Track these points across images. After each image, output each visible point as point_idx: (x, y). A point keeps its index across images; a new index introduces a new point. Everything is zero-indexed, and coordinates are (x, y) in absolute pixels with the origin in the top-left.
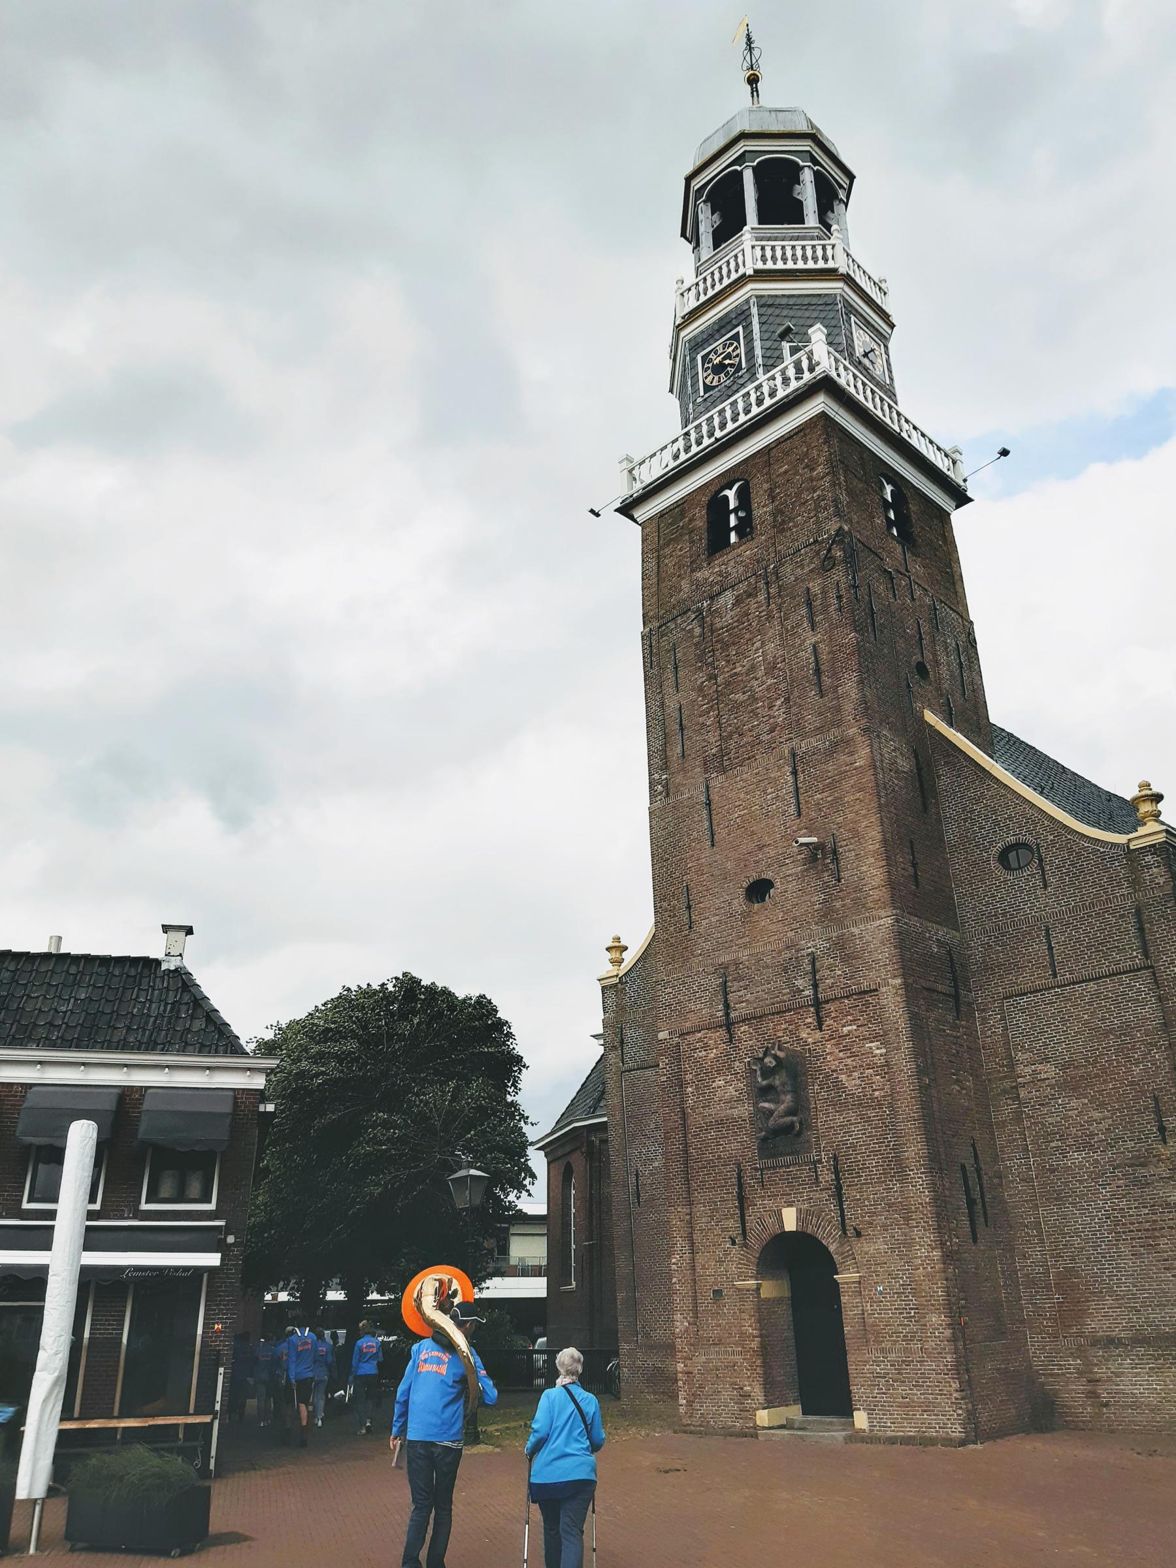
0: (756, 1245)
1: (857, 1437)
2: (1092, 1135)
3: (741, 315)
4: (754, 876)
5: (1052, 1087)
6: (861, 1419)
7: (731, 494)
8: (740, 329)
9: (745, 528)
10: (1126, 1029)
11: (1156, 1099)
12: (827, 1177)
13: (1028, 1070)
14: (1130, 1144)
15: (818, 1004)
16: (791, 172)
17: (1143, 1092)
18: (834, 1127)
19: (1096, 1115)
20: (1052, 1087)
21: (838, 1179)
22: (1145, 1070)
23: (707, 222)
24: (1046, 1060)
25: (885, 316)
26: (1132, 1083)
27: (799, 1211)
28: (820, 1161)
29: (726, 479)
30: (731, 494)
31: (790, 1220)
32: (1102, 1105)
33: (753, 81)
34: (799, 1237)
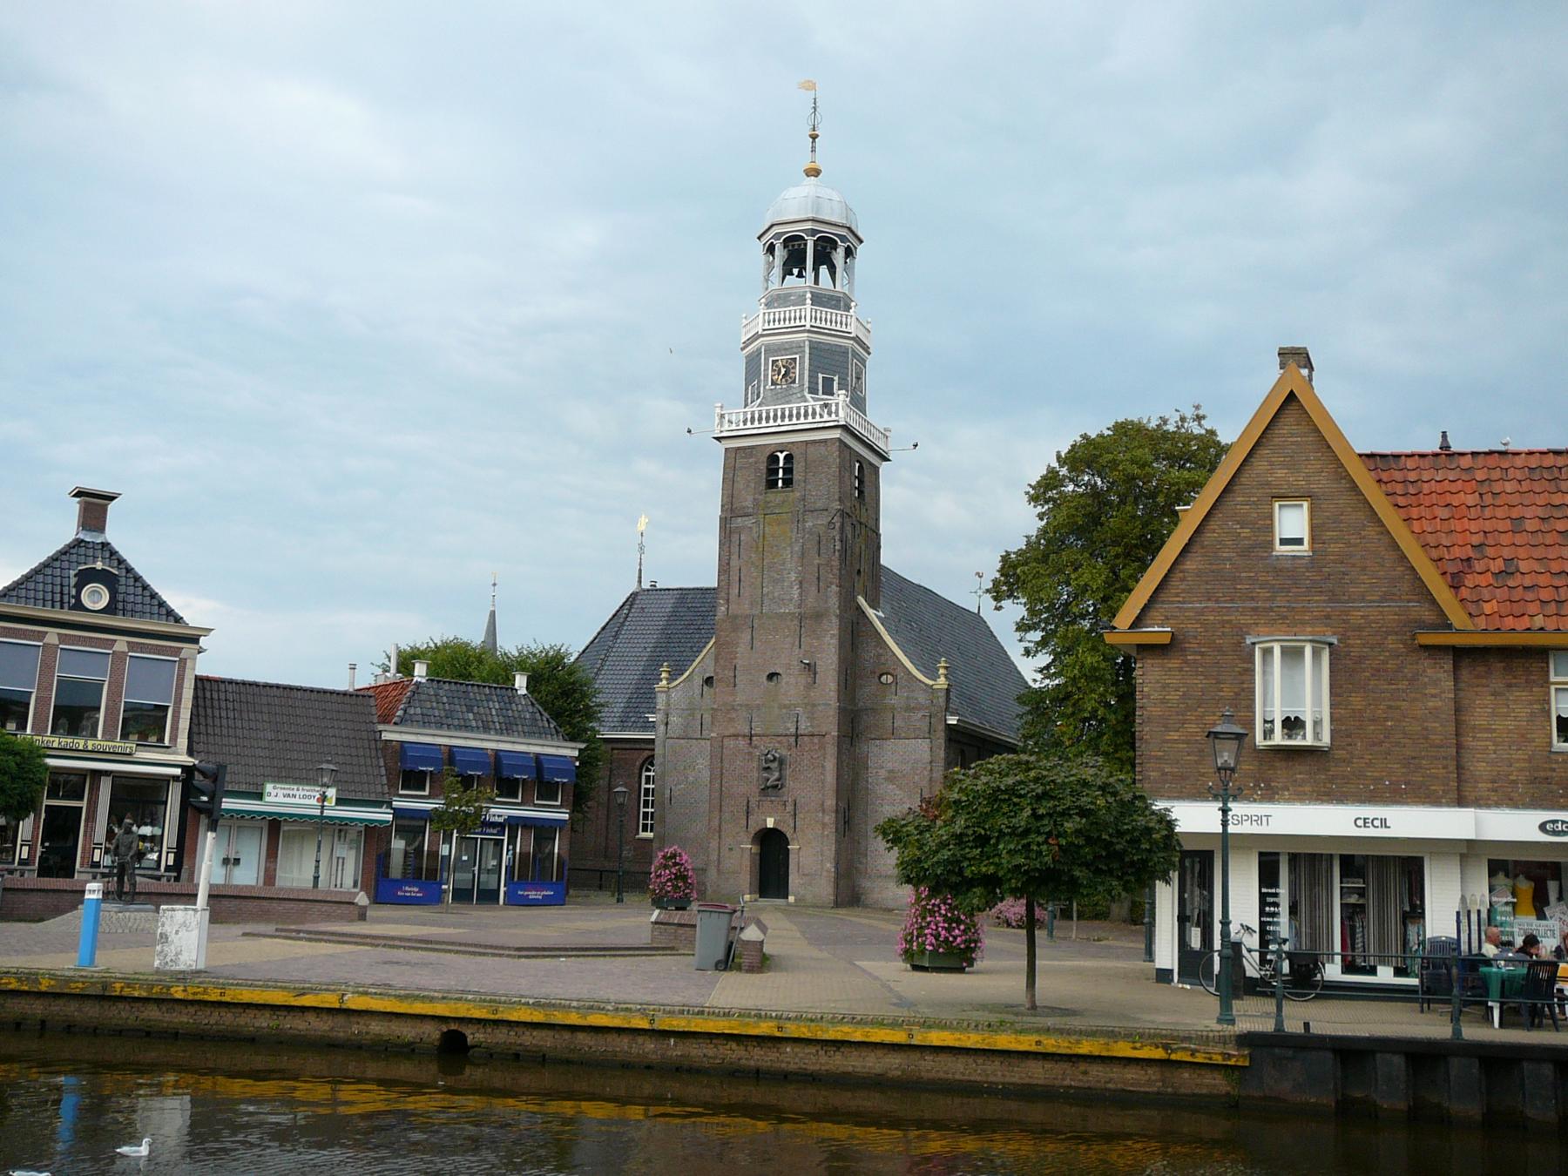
0: (753, 830)
1: (789, 905)
3: (798, 347)
6: (791, 899)
7: (781, 456)
9: (788, 482)
12: (790, 808)
15: (797, 736)
16: (834, 246)
18: (796, 787)
23: (780, 253)
25: (867, 349)
30: (781, 456)
31: (770, 823)
33: (814, 137)
34: (774, 832)
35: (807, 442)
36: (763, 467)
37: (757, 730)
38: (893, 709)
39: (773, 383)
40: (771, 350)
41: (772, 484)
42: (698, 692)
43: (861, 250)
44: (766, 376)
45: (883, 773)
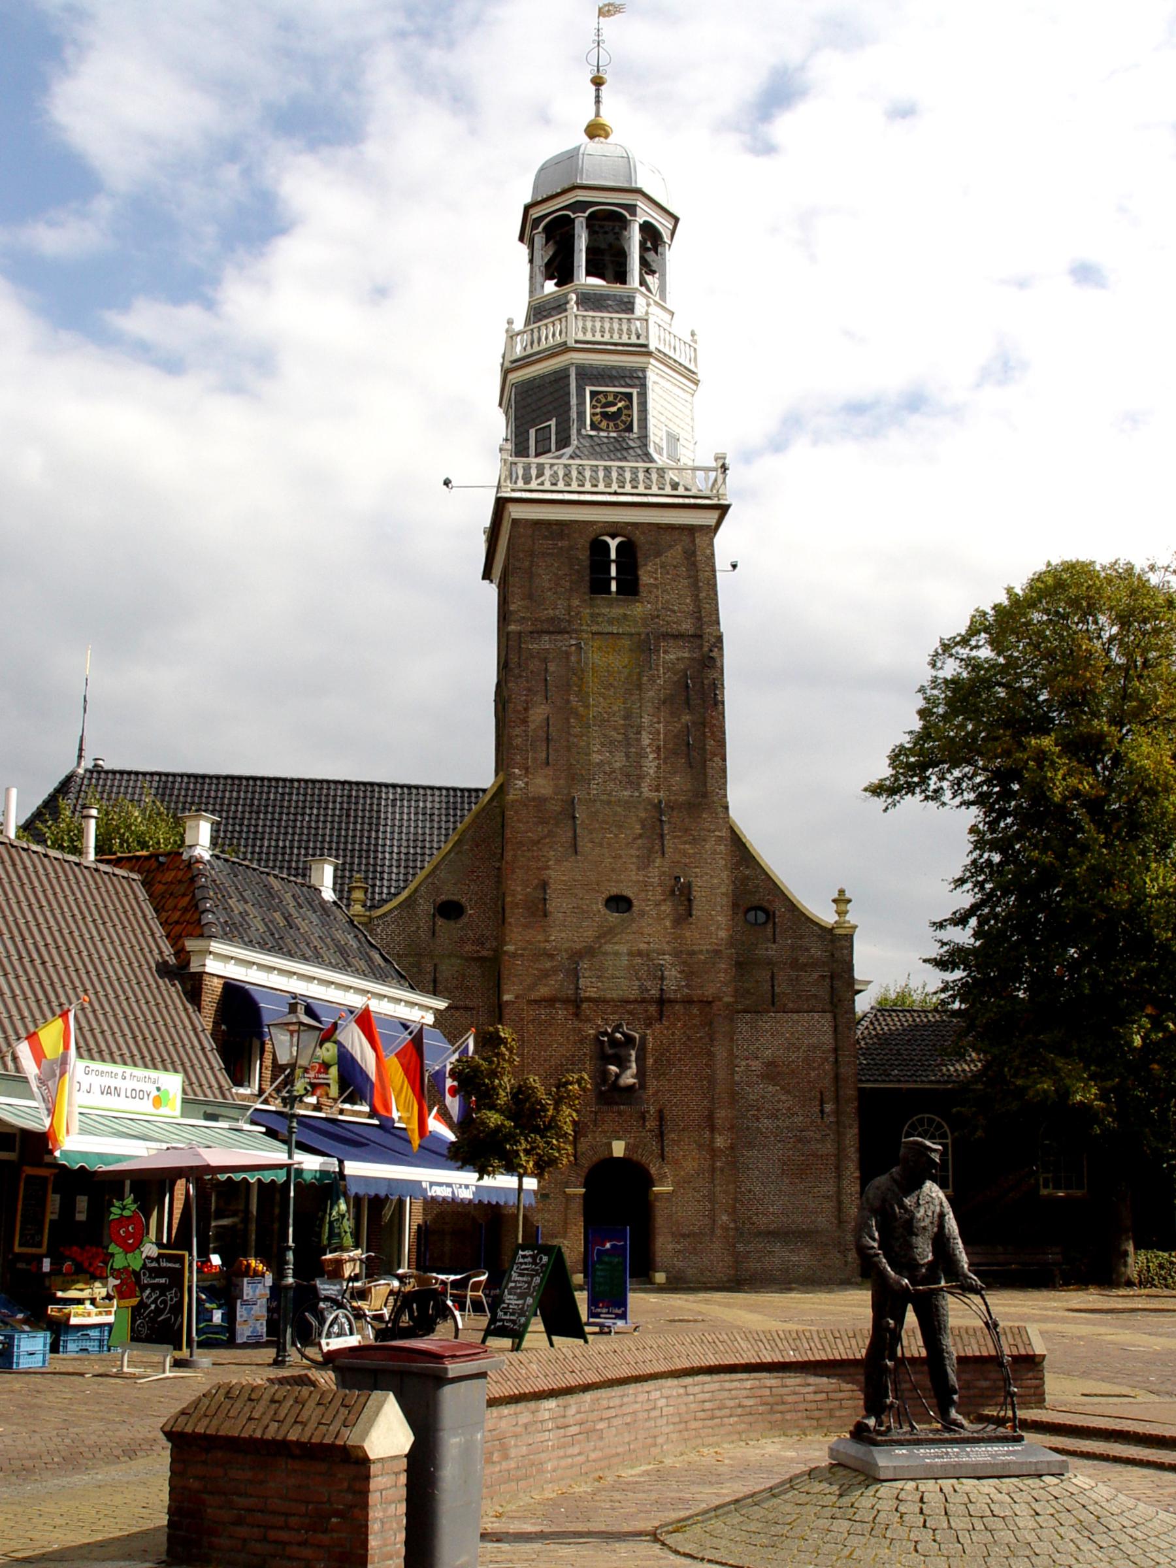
0: (586, 1163)
2: (778, 1110)
4: (614, 891)
5: (758, 1076)
7: (613, 544)
8: (635, 391)
9: (630, 587)
10: (814, 1047)
11: (821, 1093)
12: (651, 1124)
13: (744, 1063)
14: (801, 1118)
17: (815, 1087)
19: (784, 1098)
20: (758, 1076)
21: (661, 1126)
22: (819, 1075)
24: (757, 1058)
26: (809, 1082)
27: (627, 1145)
28: (648, 1112)
29: (614, 530)
30: (613, 544)
31: (618, 1149)
32: (788, 1092)
33: (598, 82)
35: (658, 526)
36: (584, 556)
37: (592, 993)
38: (770, 963)
39: (594, 426)
40: (587, 375)
41: (599, 586)
42: (424, 926)
43: (675, 256)
44: (581, 415)
45: (756, 1065)
